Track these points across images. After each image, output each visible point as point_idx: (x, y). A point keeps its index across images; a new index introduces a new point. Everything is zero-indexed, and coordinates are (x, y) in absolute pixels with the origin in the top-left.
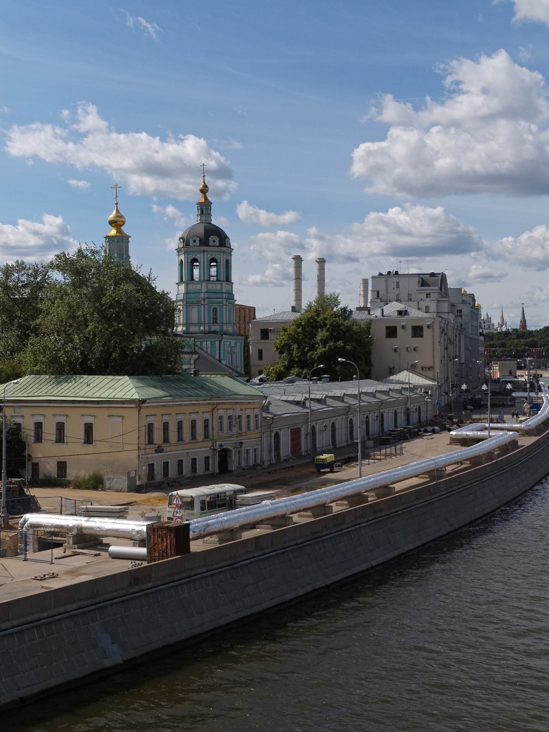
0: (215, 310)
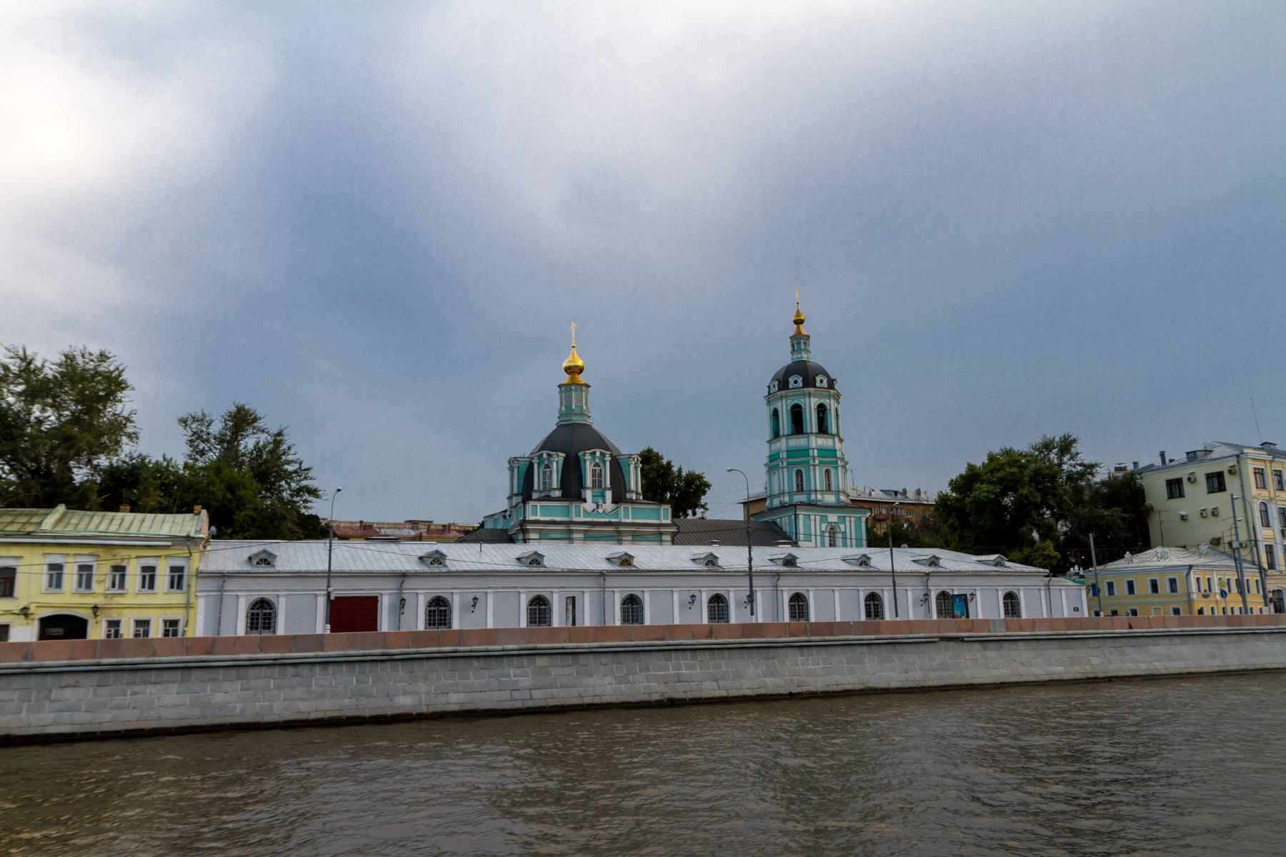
0: (799, 473)
